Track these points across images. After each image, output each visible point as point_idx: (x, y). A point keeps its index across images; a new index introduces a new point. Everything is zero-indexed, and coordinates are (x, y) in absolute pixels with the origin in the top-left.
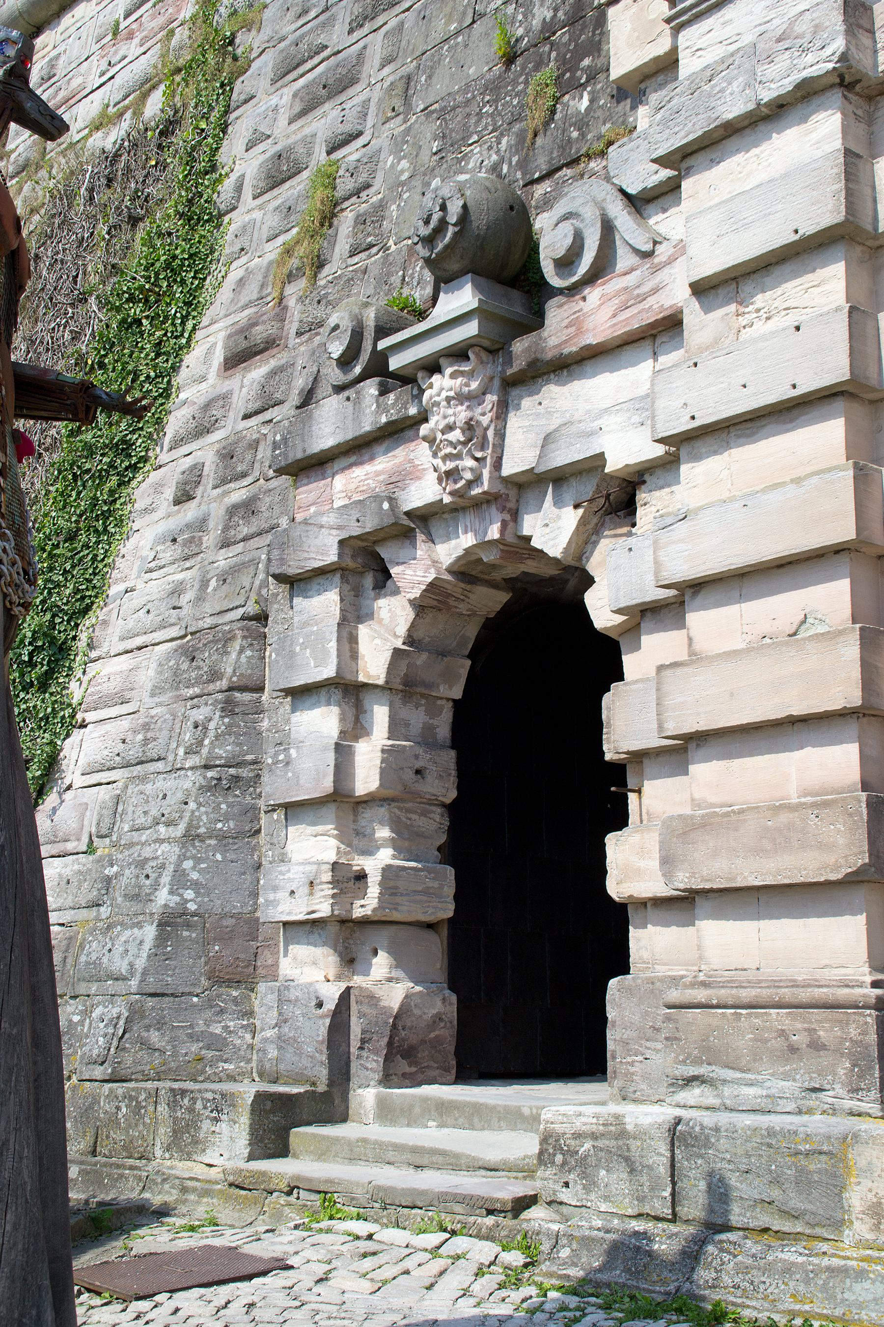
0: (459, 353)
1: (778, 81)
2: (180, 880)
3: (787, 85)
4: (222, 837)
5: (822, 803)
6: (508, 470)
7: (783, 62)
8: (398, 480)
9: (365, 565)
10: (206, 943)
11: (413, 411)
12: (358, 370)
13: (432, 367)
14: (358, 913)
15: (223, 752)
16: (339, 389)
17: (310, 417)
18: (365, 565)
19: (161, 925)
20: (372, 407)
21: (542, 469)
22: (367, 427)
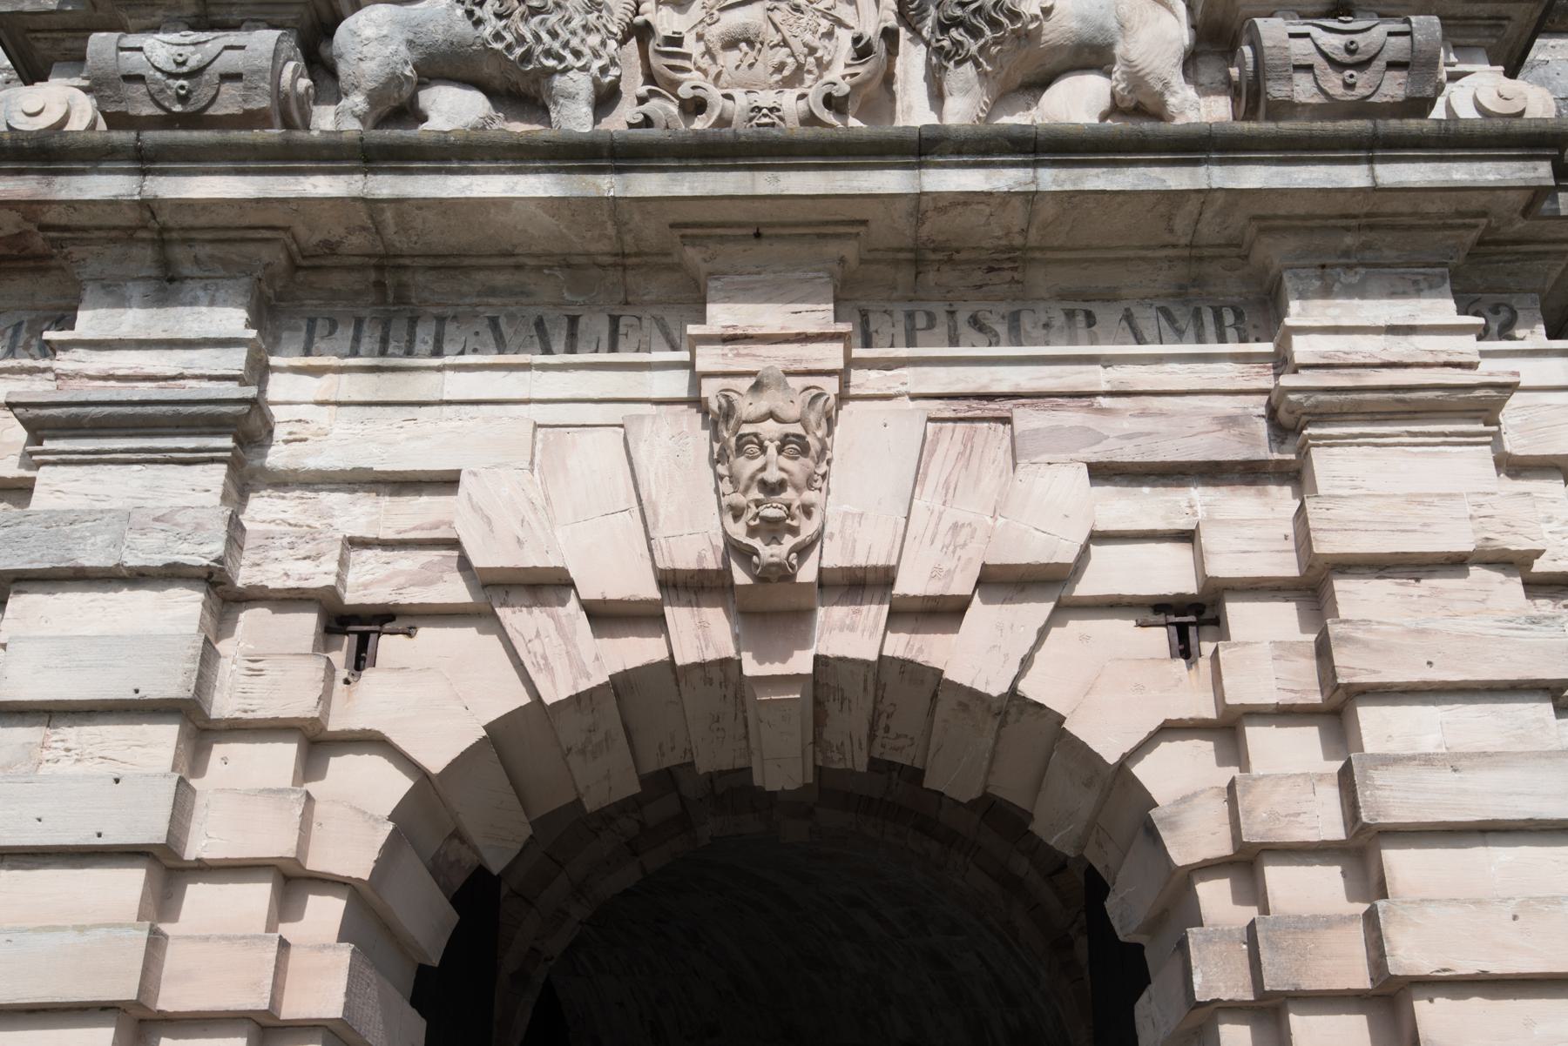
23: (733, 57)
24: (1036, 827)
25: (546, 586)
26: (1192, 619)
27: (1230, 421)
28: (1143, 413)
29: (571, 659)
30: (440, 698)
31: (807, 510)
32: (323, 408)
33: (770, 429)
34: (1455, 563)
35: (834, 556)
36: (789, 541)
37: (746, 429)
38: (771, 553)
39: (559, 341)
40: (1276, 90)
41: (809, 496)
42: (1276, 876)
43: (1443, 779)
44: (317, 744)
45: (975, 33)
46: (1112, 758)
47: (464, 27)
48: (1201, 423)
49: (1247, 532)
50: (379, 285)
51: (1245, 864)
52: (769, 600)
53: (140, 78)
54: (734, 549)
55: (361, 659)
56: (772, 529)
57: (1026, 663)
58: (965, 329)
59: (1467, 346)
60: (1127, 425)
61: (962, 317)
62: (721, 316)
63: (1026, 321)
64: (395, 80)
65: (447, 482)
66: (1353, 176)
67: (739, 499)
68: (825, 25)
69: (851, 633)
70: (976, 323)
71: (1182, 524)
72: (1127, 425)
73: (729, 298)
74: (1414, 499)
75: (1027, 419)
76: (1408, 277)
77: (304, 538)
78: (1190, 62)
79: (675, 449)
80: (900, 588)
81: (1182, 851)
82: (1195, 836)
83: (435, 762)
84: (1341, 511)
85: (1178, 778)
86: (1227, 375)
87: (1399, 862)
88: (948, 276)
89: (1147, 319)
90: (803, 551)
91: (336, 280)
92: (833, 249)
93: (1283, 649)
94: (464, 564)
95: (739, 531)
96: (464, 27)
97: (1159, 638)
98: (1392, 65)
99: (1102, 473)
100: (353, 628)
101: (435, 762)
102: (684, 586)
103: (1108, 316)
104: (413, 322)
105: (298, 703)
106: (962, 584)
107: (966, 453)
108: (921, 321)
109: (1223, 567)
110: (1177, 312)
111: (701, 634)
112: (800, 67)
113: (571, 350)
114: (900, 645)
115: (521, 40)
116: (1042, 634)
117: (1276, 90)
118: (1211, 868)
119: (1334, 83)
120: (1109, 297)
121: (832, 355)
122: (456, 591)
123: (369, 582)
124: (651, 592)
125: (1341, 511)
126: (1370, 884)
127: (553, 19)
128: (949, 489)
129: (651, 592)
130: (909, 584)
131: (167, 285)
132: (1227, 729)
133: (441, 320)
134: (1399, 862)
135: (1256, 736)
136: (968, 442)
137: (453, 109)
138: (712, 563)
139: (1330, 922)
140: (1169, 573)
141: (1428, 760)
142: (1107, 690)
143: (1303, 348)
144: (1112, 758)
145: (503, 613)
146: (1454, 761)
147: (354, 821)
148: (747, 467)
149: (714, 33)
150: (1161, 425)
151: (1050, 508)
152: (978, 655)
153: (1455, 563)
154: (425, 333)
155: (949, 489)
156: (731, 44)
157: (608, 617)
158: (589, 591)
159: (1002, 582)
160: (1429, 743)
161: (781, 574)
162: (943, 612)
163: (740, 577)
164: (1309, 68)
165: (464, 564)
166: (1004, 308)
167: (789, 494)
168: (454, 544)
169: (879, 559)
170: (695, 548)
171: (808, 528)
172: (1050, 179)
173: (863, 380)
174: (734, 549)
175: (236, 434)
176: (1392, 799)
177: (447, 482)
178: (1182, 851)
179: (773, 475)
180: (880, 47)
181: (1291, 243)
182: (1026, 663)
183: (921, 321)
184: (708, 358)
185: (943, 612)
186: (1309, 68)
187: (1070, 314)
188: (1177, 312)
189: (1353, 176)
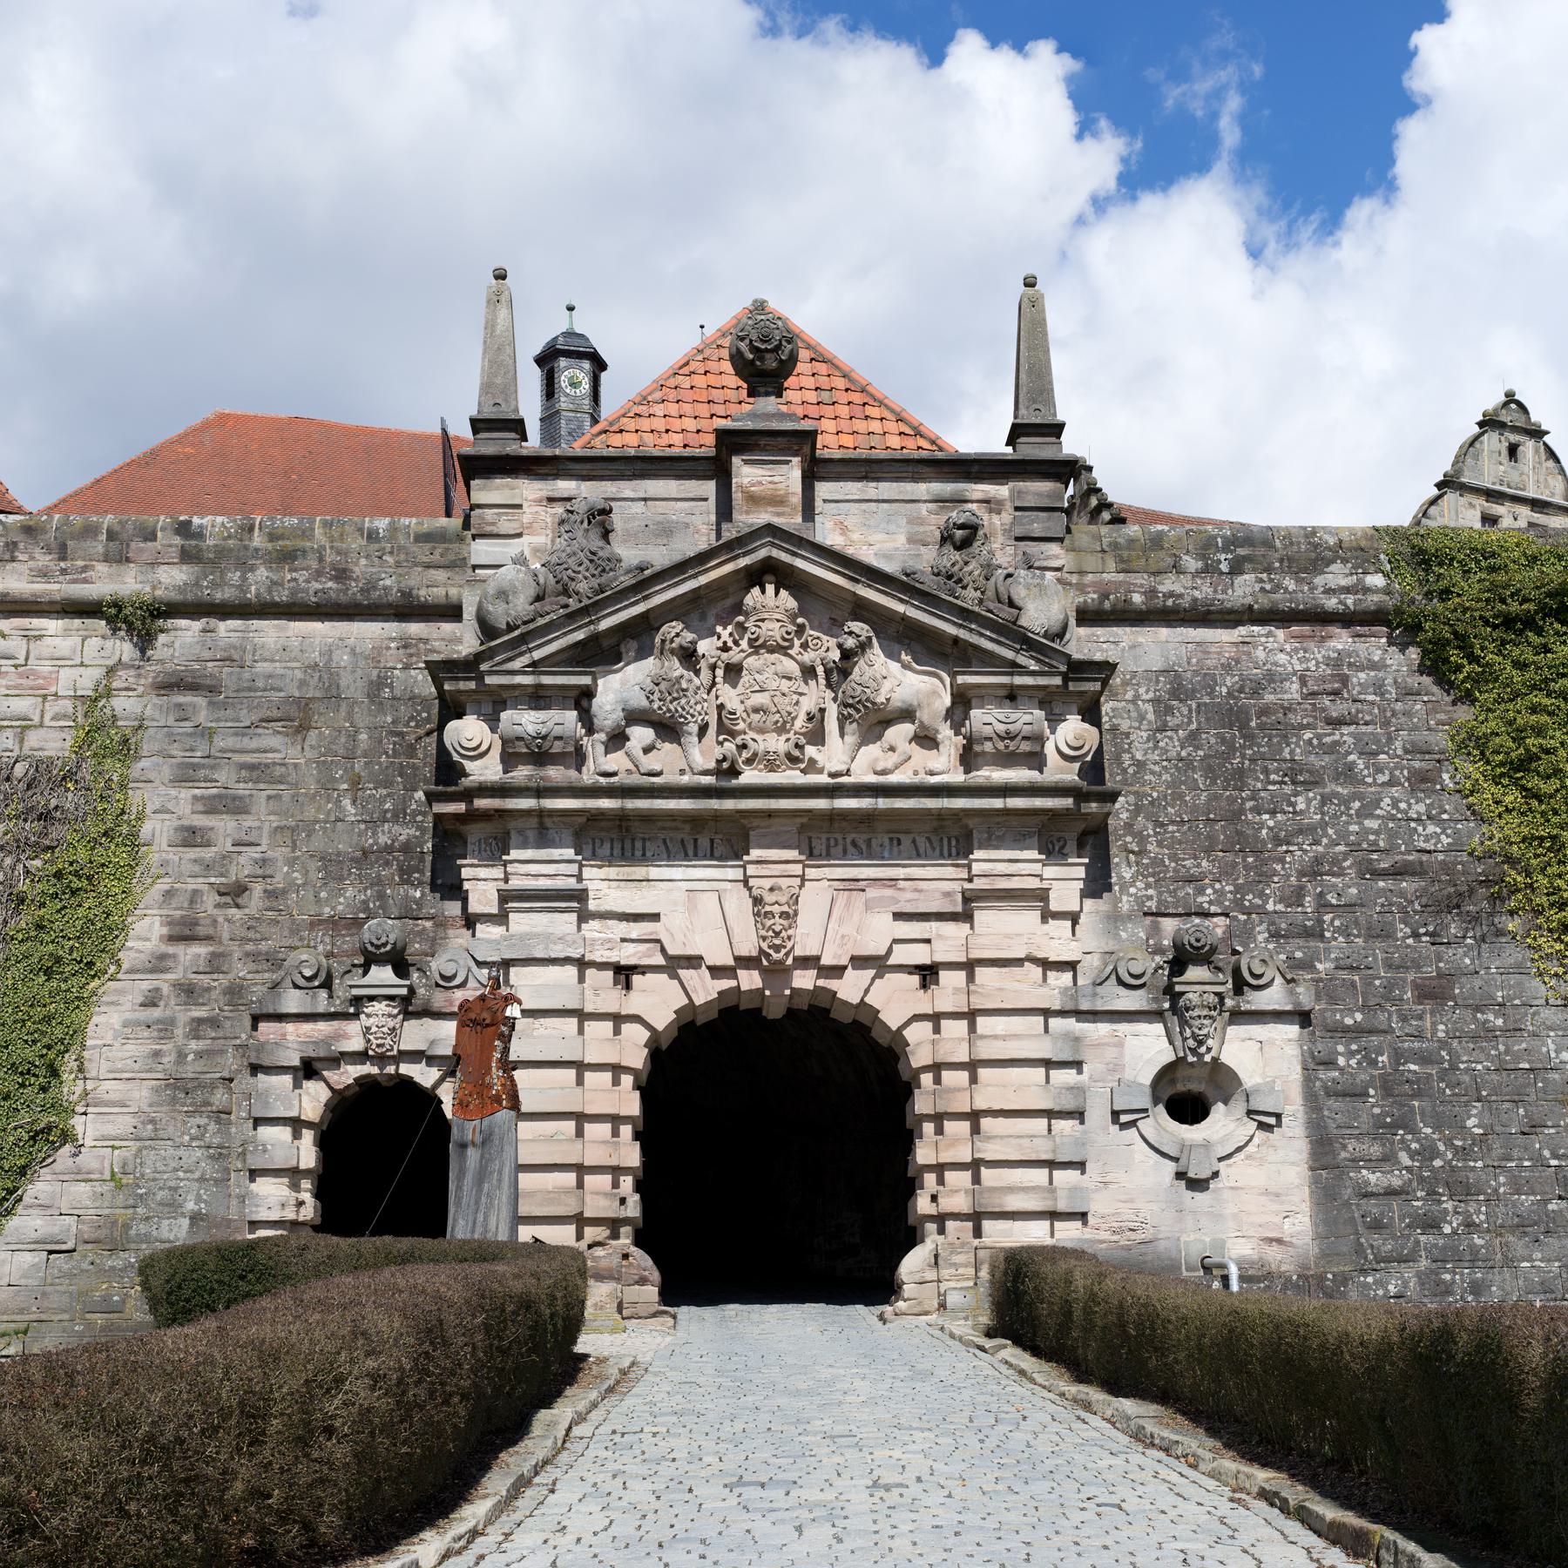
0: (391, 998)
1: (558, 951)
2: (199, 1199)
3: (562, 955)
4: (216, 1180)
5: (566, 1191)
6: (402, 1047)
7: (560, 947)
8: (338, 1036)
9: (308, 1070)
10: (210, 1228)
11: (352, 1010)
12: (316, 983)
13: (372, 998)
14: (301, 1219)
15: (216, 1141)
16: (296, 986)
17: (279, 994)
18: (308, 1070)
19: (191, 1218)
20: (322, 1002)
21: (429, 1053)
22: (321, 1010)
23: (756, 717)
24: (873, 1034)
25: (693, 961)
26: (928, 974)
27: (947, 894)
28: (916, 890)
29: (705, 989)
30: (659, 1002)
31: (789, 938)
32: (607, 886)
33: (776, 909)
34: (1018, 962)
35: (798, 952)
36: (784, 951)
37: (768, 908)
38: (775, 956)
39: (691, 852)
40: (977, 748)
41: (790, 932)
42: (945, 1074)
43: (1000, 1043)
44: (618, 1019)
45: (858, 711)
46: (894, 1028)
47: (645, 703)
48: (937, 895)
49: (949, 941)
50: (620, 826)
51: (937, 1068)
52: (776, 972)
53: (522, 739)
54: (761, 950)
55: (628, 986)
56: (777, 948)
57: (867, 991)
58: (850, 848)
59: (1036, 868)
60: (909, 895)
61: (848, 841)
62: (755, 853)
63: (874, 842)
64: (619, 726)
65: (655, 917)
66: (997, 803)
67: (763, 933)
68: (795, 697)
69: (804, 980)
70: (854, 844)
71: (926, 936)
72: (909, 895)
73: (760, 847)
74: (1007, 936)
75: (872, 893)
76: (1019, 841)
77: (609, 944)
78: (949, 714)
79: (738, 903)
80: (823, 962)
81: (916, 1063)
82: (919, 1057)
83: (660, 1027)
84: (981, 941)
85: (917, 1034)
86: (950, 872)
87: (983, 1073)
88: (844, 824)
89: (922, 842)
90: (787, 954)
91: (603, 824)
92: (799, 820)
93: (956, 990)
94: (663, 950)
95: (764, 946)
96: (645, 703)
97: (915, 980)
98: (1024, 738)
99: (898, 916)
100: (624, 974)
101: (660, 1027)
102: (744, 962)
103: (906, 841)
104: (633, 840)
105: (613, 1009)
106: (844, 961)
107: (848, 904)
108: (832, 843)
109: (939, 958)
110: (934, 839)
111: (750, 980)
112: (785, 722)
113: (696, 855)
114: (821, 983)
115: (669, 710)
116: (873, 980)
117: (977, 748)
118: (926, 1069)
119: (1001, 746)
120: (907, 832)
121: (798, 869)
122: (659, 960)
123: (628, 955)
124: (731, 962)
125: (981, 941)
126: (974, 1080)
127: (683, 701)
128: (841, 920)
129: (731, 962)
130: (825, 961)
131: (543, 841)
132: (936, 1018)
133: (644, 840)
134: (983, 1073)
135: (944, 1023)
136: (849, 898)
137: (641, 735)
138: (754, 953)
139: (959, 1090)
140: (920, 955)
141: (996, 1037)
142: (894, 1001)
143: (977, 868)
144: (894, 1028)
145: (680, 972)
146: (1004, 1038)
147: (633, 1049)
148: (769, 923)
149: (749, 703)
150: (922, 896)
151: (878, 932)
152: (849, 988)
153: (1018, 962)
154: (638, 845)
155: (841, 920)
156: (756, 710)
157: (717, 971)
158: (709, 963)
159: (860, 962)
160: (999, 1030)
161: (781, 962)
162: (837, 971)
163: (765, 963)
164: (991, 739)
165: (663, 950)
166: (865, 836)
167: (784, 934)
168: (658, 941)
169: (814, 953)
170: (748, 948)
171: (789, 945)
172: (883, 803)
173: (811, 873)
174: (761, 950)
175: (575, 899)
176: (986, 1051)
177: (655, 917)
178: (916, 1063)
179: (778, 928)
180: (818, 716)
181: (976, 820)
182: (867, 991)
183: (832, 843)
184: (751, 870)
185: (837, 971)
186: (991, 739)
187: (891, 839)
188: (934, 839)
189: (997, 803)
